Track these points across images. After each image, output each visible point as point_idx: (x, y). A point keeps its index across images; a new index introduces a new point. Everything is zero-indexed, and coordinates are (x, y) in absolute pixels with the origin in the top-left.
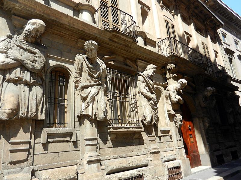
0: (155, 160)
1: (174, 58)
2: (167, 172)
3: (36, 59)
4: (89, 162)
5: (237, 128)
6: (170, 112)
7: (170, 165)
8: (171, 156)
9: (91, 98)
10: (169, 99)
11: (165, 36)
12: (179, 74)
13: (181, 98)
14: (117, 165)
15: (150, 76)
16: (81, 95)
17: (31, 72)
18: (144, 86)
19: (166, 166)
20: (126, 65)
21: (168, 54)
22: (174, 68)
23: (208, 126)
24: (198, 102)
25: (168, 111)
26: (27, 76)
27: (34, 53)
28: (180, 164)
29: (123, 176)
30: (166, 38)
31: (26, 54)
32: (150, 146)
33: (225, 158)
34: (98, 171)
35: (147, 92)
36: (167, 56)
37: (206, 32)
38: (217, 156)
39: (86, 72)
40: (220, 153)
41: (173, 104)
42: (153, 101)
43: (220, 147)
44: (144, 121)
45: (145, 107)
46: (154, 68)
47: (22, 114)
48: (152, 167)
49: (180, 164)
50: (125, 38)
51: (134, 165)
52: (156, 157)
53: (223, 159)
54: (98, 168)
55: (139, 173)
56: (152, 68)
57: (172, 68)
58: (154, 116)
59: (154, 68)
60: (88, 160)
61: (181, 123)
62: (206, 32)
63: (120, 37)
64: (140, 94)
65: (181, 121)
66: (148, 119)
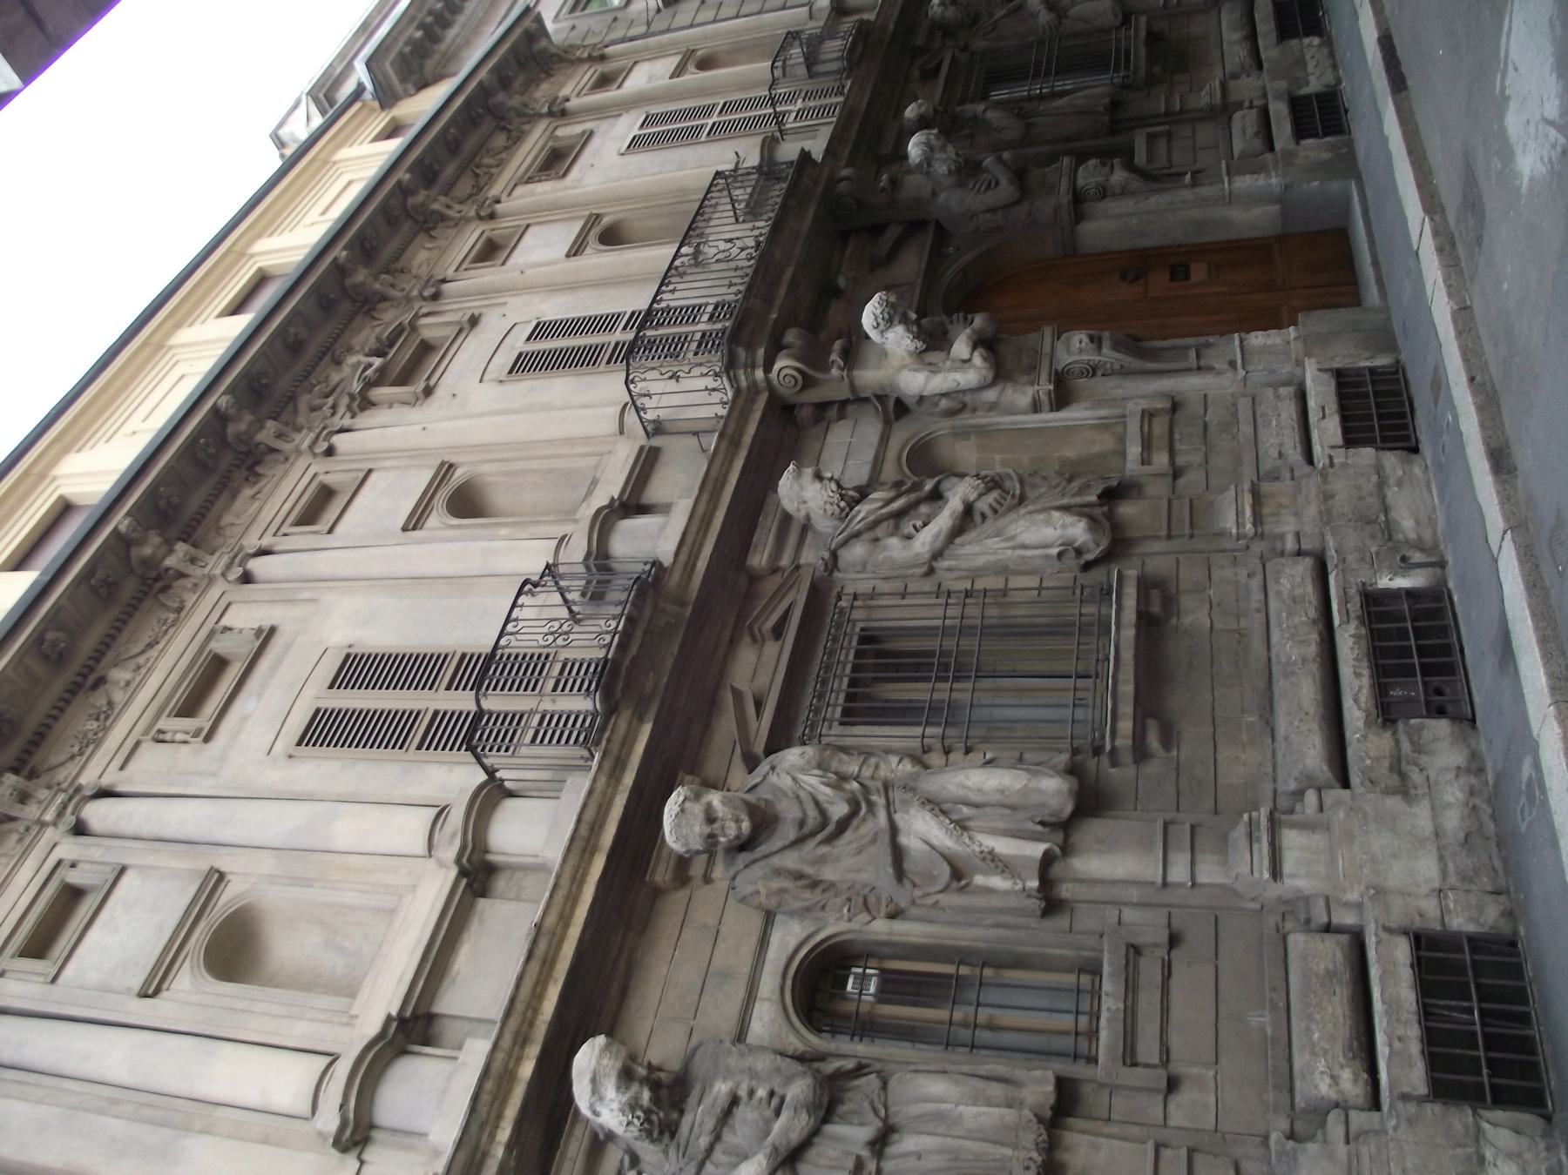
0: (1296, 514)
1: (741, 353)
2: (1366, 454)
3: (761, 1093)
6: (1044, 398)
7: (1327, 430)
8: (1284, 416)
9: (958, 839)
10: (968, 398)
11: (608, 386)
13: (968, 331)
14: (1304, 727)
15: (843, 504)
16: (939, 888)
17: (826, 1120)
18: (894, 542)
19: (1331, 458)
20: (778, 632)
21: (715, 385)
22: (797, 359)
23: (1125, 174)
24: (988, 216)
25: (1036, 407)
27: (734, 1101)
28: (1326, 370)
30: (629, 391)
32: (1223, 534)
33: (1314, 84)
34: (1327, 828)
35: (933, 528)
36: (730, 395)
37: (564, 113)
39: (822, 860)
40: (1280, 111)
41: (1001, 373)
43: (1251, 107)
44: (1090, 557)
45: (1014, 548)
46: (798, 474)
47: (1027, 1168)
48: (1331, 542)
49: (1326, 370)
50: (639, 634)
51: (1315, 636)
52: (1281, 505)
53: (1318, 96)
54: (1307, 826)
55: (1355, 605)
58: (1065, 501)
59: (798, 474)
60: (1266, 875)
61: (1106, 343)
62: (564, 113)
63: (635, 659)
64: (944, 564)
65: (1092, 339)
66: (1078, 530)
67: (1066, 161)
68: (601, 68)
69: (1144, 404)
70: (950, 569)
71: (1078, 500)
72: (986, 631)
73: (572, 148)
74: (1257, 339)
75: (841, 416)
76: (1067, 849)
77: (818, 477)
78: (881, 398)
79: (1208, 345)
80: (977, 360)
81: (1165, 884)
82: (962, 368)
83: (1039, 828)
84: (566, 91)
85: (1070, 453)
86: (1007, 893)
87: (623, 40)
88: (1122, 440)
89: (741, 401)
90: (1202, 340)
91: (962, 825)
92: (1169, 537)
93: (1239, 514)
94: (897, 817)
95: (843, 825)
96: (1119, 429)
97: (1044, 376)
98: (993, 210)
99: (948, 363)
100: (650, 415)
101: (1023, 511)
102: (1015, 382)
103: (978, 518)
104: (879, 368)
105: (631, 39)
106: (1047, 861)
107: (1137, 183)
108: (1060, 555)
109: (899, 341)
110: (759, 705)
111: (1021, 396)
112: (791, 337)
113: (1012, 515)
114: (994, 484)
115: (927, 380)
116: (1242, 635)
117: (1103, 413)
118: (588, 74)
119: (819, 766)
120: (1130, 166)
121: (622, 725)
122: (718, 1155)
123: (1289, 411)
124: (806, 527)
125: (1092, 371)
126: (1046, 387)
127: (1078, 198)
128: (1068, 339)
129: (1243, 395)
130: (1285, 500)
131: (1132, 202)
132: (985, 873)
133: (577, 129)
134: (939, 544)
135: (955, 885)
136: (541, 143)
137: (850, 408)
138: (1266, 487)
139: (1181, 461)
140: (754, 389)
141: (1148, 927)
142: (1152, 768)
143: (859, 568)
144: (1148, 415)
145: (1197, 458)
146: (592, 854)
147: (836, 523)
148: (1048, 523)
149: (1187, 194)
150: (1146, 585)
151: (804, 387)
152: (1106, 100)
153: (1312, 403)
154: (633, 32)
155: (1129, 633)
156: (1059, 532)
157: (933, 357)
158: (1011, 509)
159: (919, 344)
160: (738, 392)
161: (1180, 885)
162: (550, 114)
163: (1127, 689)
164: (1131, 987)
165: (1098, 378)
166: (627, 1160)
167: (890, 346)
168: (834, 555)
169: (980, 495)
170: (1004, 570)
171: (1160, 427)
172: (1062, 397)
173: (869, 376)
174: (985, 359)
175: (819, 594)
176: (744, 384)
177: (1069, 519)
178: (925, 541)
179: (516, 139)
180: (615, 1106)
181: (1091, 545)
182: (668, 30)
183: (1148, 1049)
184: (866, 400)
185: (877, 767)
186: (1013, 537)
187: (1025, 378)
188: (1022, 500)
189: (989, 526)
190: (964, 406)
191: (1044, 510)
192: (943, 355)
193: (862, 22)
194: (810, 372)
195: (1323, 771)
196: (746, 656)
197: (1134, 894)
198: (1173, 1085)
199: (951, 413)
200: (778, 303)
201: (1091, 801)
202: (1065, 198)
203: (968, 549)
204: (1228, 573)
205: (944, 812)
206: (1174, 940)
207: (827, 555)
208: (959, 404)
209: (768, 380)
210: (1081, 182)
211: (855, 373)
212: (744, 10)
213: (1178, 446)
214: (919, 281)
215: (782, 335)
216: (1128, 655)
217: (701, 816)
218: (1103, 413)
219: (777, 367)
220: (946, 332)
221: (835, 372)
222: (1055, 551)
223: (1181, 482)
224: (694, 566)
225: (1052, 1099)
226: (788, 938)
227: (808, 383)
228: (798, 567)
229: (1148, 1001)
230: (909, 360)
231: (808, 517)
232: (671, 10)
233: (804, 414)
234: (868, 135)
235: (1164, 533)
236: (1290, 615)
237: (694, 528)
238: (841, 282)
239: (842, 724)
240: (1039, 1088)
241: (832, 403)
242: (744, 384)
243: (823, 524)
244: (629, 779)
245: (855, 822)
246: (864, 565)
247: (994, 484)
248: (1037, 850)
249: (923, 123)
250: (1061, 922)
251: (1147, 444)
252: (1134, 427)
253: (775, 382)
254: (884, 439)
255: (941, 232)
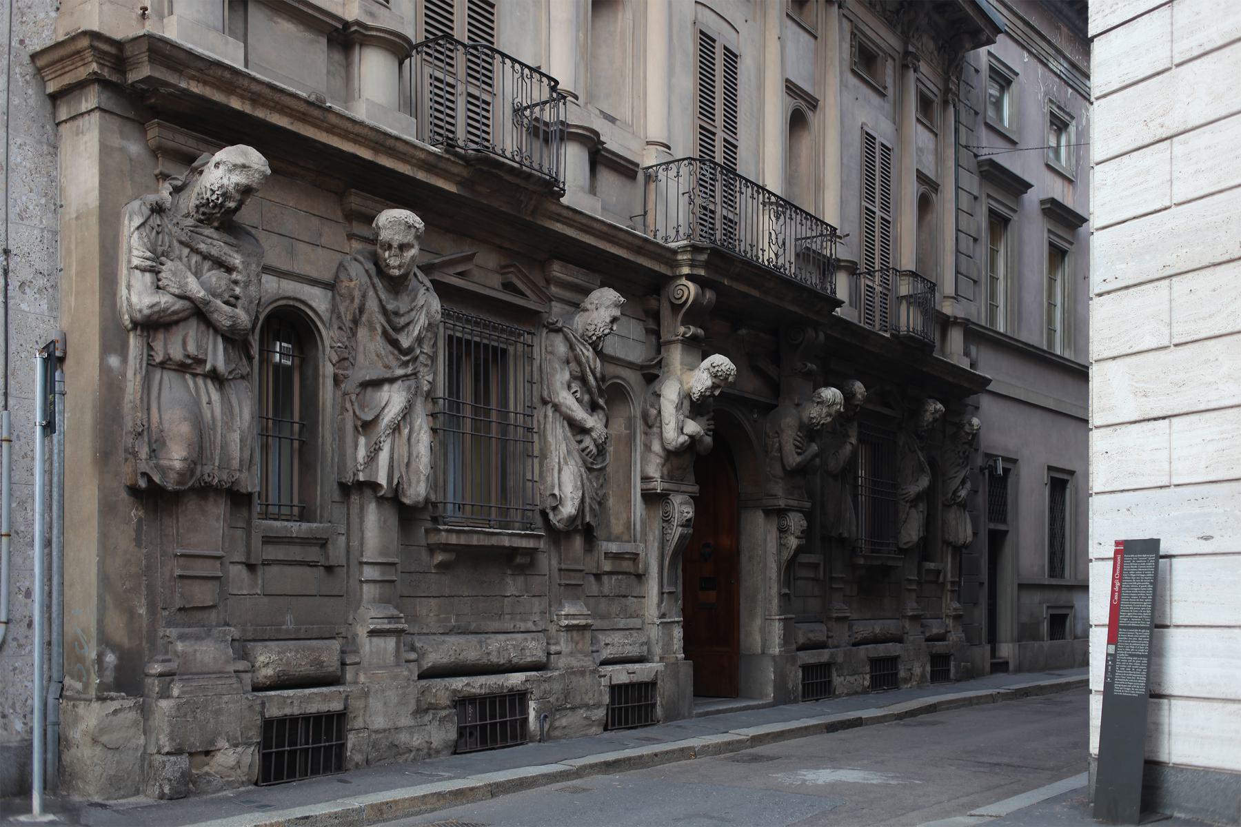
3: (238, 290)
4: (373, 633)
5: (932, 566)
6: (651, 485)
8: (630, 648)
9: (388, 426)
10: (655, 430)
11: (686, 145)
12: (712, 328)
14: (452, 652)
16: (357, 412)
17: (226, 339)
18: (567, 376)
20: (509, 287)
21: (681, 233)
25: (646, 479)
26: (217, 357)
27: (229, 269)
29: (468, 689)
30: (684, 159)
31: (215, 277)
32: (561, 605)
34: (398, 665)
36: (673, 245)
38: (806, 668)
41: (671, 455)
42: (595, 440)
44: (551, 516)
48: (556, 673)
50: (518, 181)
56: (607, 307)
57: (690, 301)
58: (587, 500)
60: (372, 627)
62: (905, 67)
66: (569, 509)
67: (808, 505)
68: (937, 101)
69: (642, 555)
70: (546, 416)
71: (587, 509)
72: (504, 443)
73: (873, 76)
74: (678, 633)
75: (648, 331)
76: (381, 500)
77: (614, 320)
78: (659, 364)
79: (676, 601)
80: (682, 439)
81: (361, 563)
82: (676, 428)
83: (395, 482)
84: (923, 67)
85: (611, 502)
86: (356, 459)
87: (957, 121)
88: (618, 539)
89: (668, 255)
90: (681, 596)
91: (396, 429)
92: (560, 570)
93: (573, 616)
94: (400, 382)
95: (395, 343)
96: (626, 537)
97: (667, 486)
98: (780, 450)
99: (682, 417)
100: (662, 175)
101: (583, 470)
102: (663, 466)
103: (579, 438)
104: (682, 364)
105: (957, 130)
106: (375, 486)
107: (786, 555)
108: (554, 495)
109: (700, 381)
110: (461, 275)
111: (654, 470)
112: (709, 295)
113: (580, 463)
114: (601, 450)
115: (671, 401)
116: (500, 616)
117: (638, 527)
118: (933, 88)
119: (429, 324)
120: (800, 549)
121: (455, 170)
122: (195, 258)
123: (633, 651)
124: (577, 306)
125: (667, 520)
126: (658, 486)
127: (781, 513)
128: (689, 503)
129: (643, 622)
130: (580, 646)
131: (774, 550)
132: (367, 444)
133: (889, 82)
134: (564, 409)
135: (359, 423)
136: (883, 45)
137: (653, 339)
138: (588, 635)
139: (605, 579)
140: (675, 264)
141: (337, 553)
142: (424, 555)
143: (549, 349)
144: (634, 557)
145: (606, 590)
146: (373, 149)
147: (580, 331)
148: (575, 487)
149: (775, 590)
150: (532, 552)
151: (672, 304)
152: (846, 535)
153: (637, 666)
154: (963, 130)
155: (506, 542)
156: (569, 495)
157: (687, 404)
158: (584, 462)
159: (696, 397)
160: (675, 252)
161: (361, 573)
162: (907, 53)
163: (475, 540)
164: (305, 541)
165: (662, 524)
166: (179, 183)
167: (701, 375)
168: (559, 330)
169: (595, 440)
170: (544, 456)
171: (626, 566)
172: (650, 498)
173: (676, 356)
174: (682, 444)
175: (532, 319)
176: (680, 257)
177: (577, 502)
178: (568, 399)
179: (890, 19)
180: (225, 181)
181: (559, 517)
182: (958, 165)
183: (273, 552)
184: (659, 352)
185: (426, 365)
186: (566, 463)
187: (666, 472)
188: (590, 470)
189: (575, 446)
190: (650, 427)
191: (583, 485)
192: (687, 413)
193: (932, 346)
194: (684, 310)
195: (427, 663)
196: (488, 259)
197: (355, 543)
198: (251, 567)
199: (645, 417)
200: (735, 285)
201: (408, 516)
202: (782, 503)
203: (559, 431)
204: (536, 609)
205: (404, 417)
206: (329, 569)
207: (559, 325)
208: (652, 423)
209: (681, 276)
210: (791, 515)
211: (679, 346)
212: (961, 235)
213: (614, 577)
214: (736, 392)
215: (711, 288)
216: (494, 541)
217: (406, 241)
218: (638, 527)
219: (690, 284)
220: (702, 415)
221: (682, 329)
222: (556, 492)
223: (592, 579)
224: (558, 221)
225: (243, 490)
226: (318, 300)
227: (676, 308)
228: (551, 300)
229: (296, 553)
230: (686, 387)
231: (586, 310)
232: (973, 167)
233: (653, 303)
234: (846, 351)
235: (563, 567)
236: (514, 646)
237: (584, 221)
238: (743, 332)
239: (450, 337)
240: (250, 482)
241: (659, 325)
242: (680, 257)
243: (579, 321)
244: (421, 176)
245: (396, 352)
246: (551, 353)
247: (601, 450)
248: (382, 480)
249: (849, 396)
250: (336, 496)
251: (617, 557)
252: (628, 548)
253: (679, 282)
254: (630, 365)
255: (768, 409)
